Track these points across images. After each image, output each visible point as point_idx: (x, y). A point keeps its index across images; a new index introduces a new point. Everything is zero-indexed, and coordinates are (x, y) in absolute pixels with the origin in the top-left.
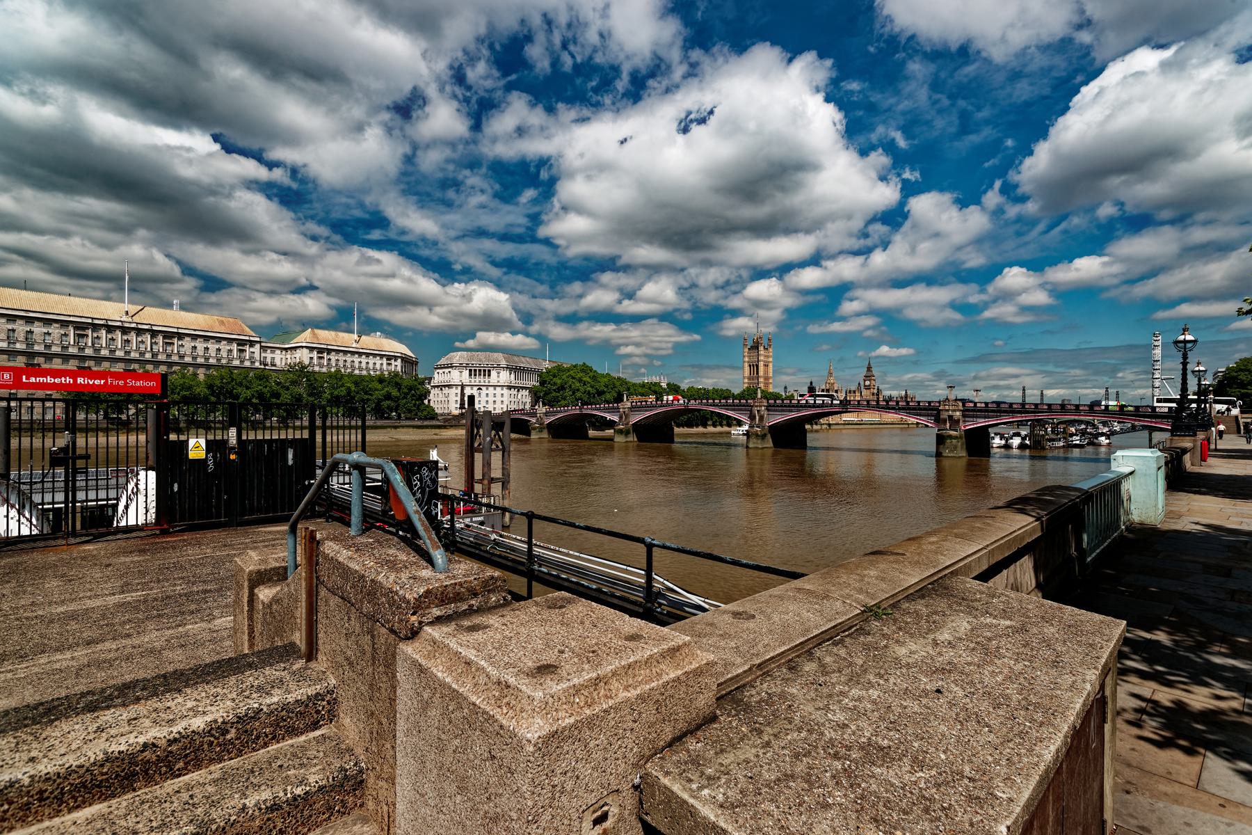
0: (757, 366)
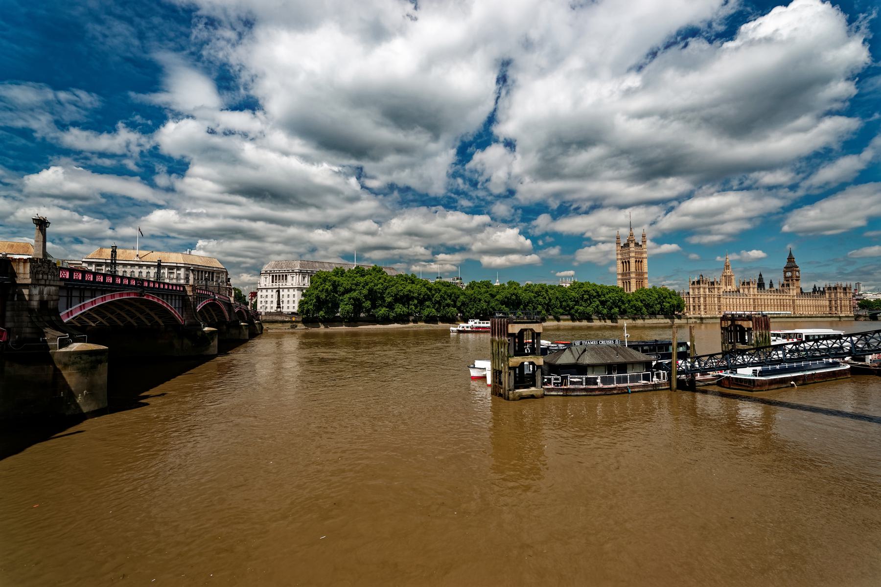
0: (629, 262)
